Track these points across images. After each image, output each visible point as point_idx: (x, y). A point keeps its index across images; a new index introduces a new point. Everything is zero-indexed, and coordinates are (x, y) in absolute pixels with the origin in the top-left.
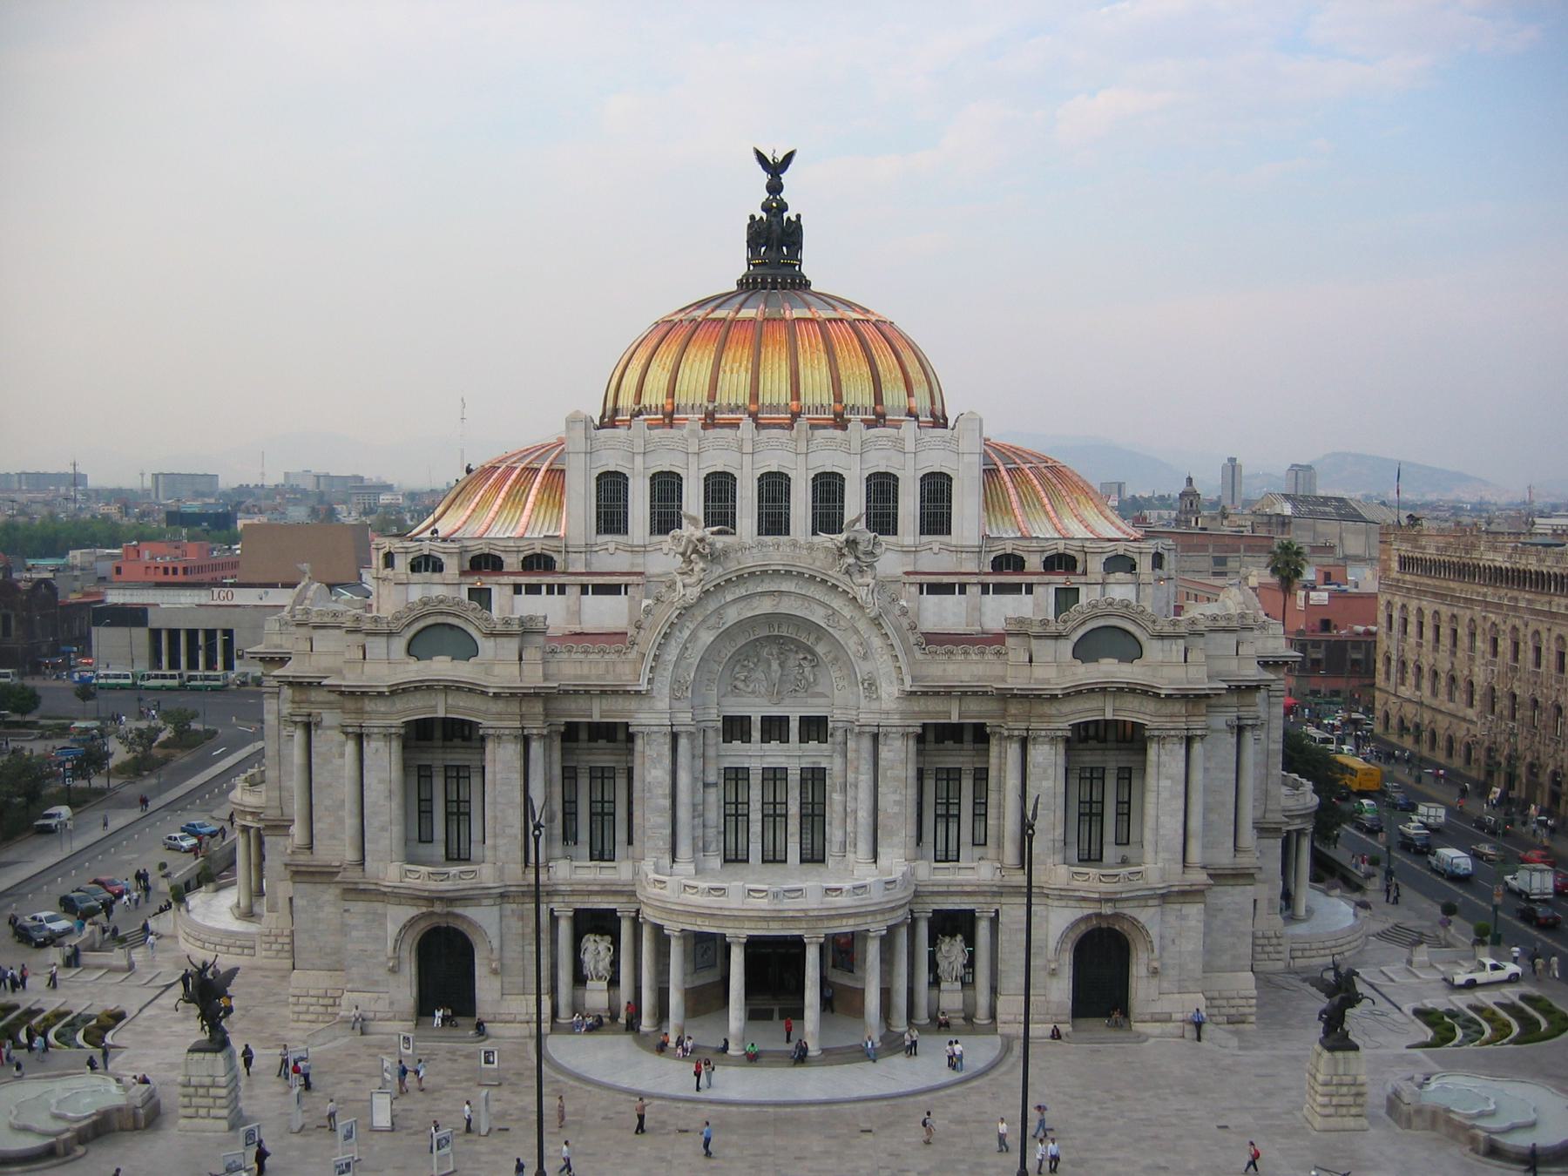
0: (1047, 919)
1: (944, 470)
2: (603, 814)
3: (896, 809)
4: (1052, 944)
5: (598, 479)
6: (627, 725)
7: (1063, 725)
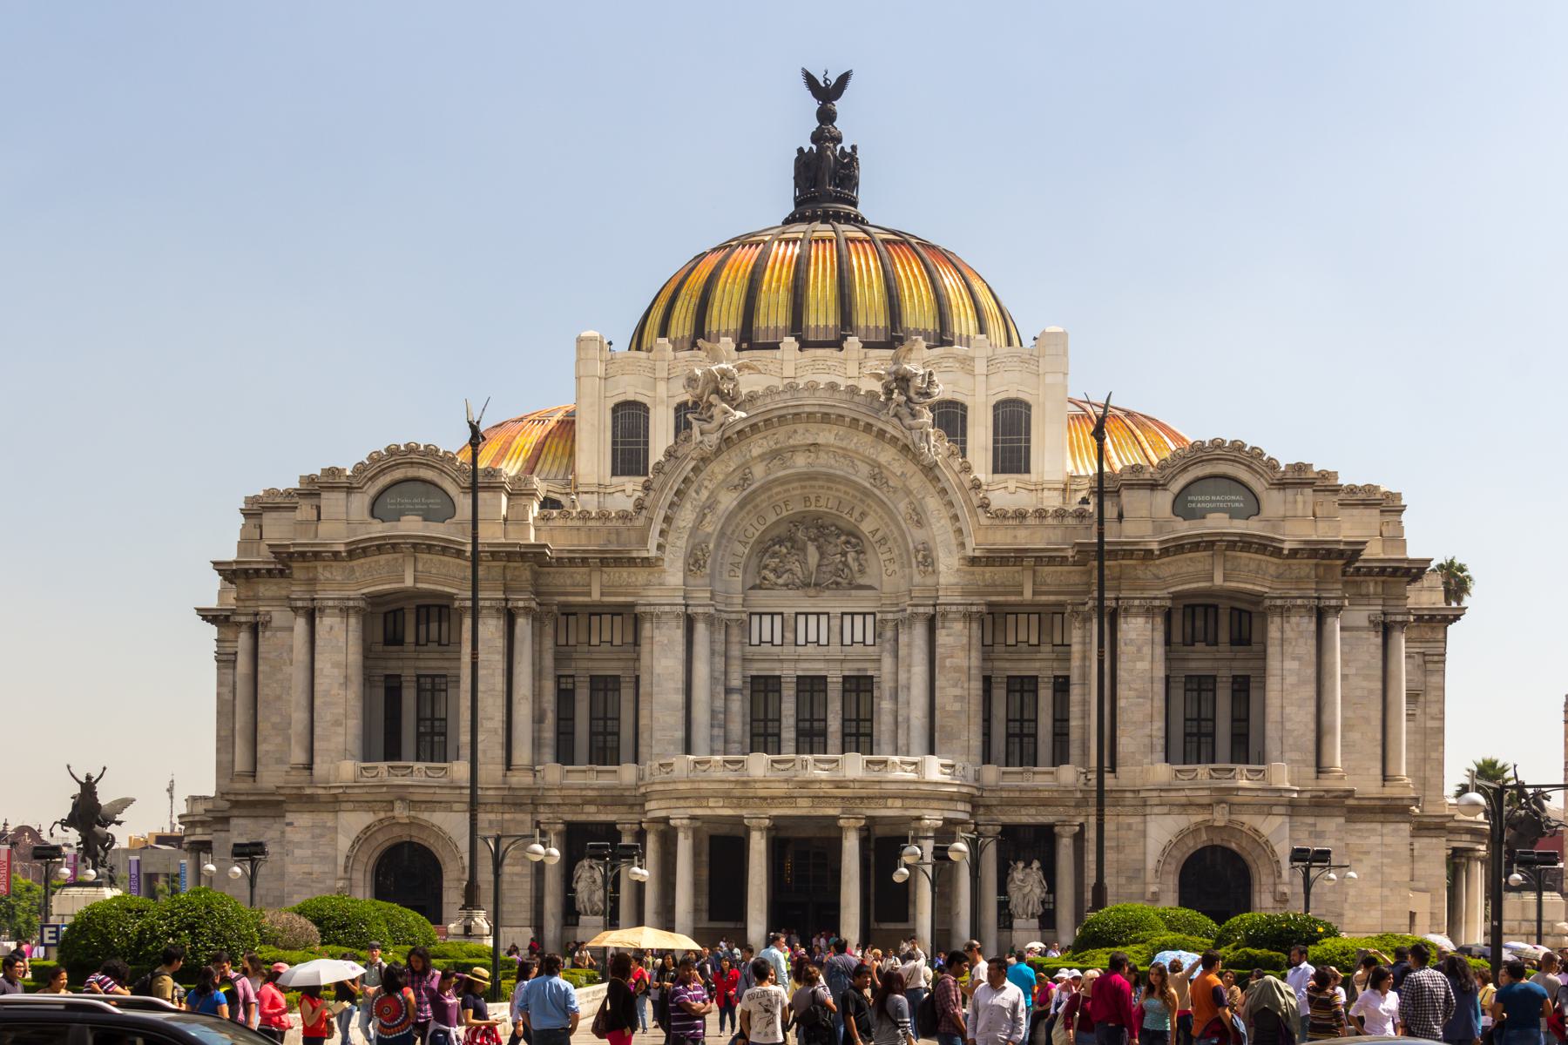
0: (1144, 834)
1: (1022, 396)
2: (605, 733)
3: (957, 706)
4: (1151, 863)
5: (615, 409)
6: (633, 605)
7: (1160, 595)
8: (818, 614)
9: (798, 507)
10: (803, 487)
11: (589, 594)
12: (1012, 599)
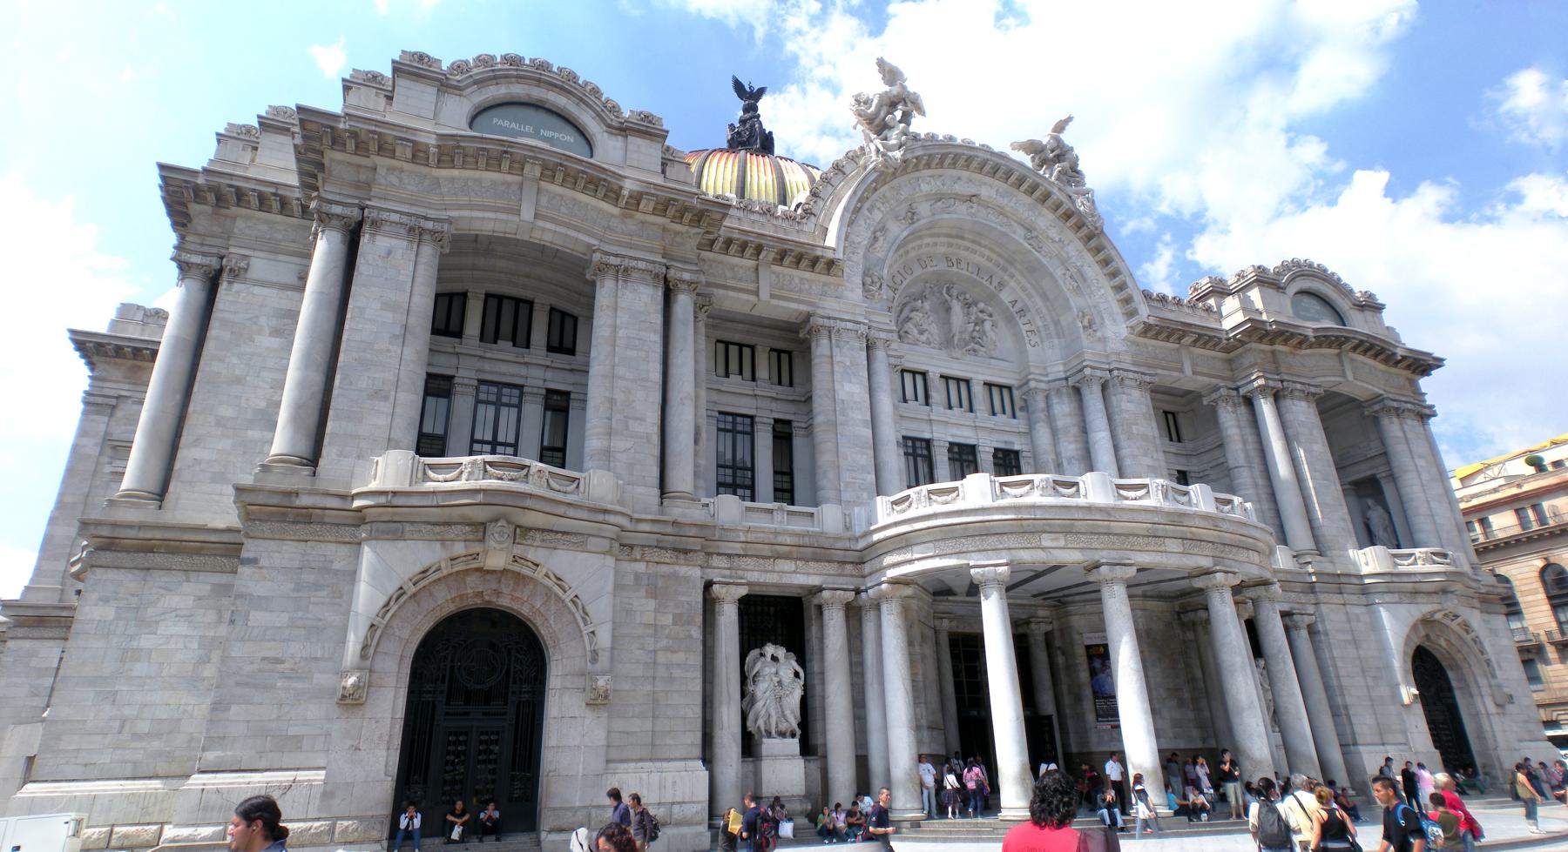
0: (1376, 627)
6: (809, 316)
9: (942, 266)
10: (950, 245)
11: (757, 293)
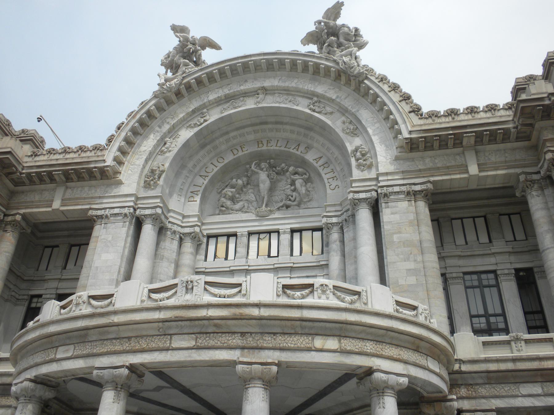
3: (412, 280)
8: (269, 232)
9: (254, 149)
10: (255, 132)
11: (51, 206)
12: (458, 176)
